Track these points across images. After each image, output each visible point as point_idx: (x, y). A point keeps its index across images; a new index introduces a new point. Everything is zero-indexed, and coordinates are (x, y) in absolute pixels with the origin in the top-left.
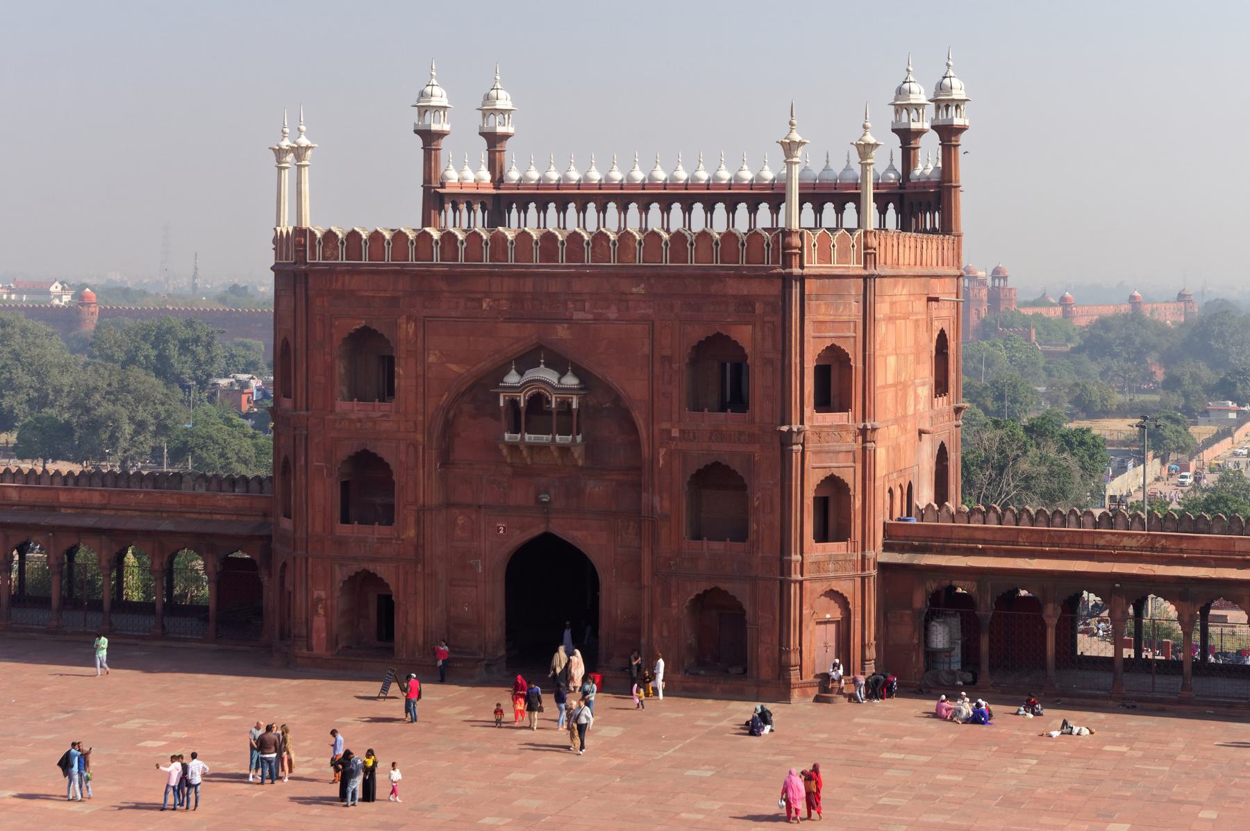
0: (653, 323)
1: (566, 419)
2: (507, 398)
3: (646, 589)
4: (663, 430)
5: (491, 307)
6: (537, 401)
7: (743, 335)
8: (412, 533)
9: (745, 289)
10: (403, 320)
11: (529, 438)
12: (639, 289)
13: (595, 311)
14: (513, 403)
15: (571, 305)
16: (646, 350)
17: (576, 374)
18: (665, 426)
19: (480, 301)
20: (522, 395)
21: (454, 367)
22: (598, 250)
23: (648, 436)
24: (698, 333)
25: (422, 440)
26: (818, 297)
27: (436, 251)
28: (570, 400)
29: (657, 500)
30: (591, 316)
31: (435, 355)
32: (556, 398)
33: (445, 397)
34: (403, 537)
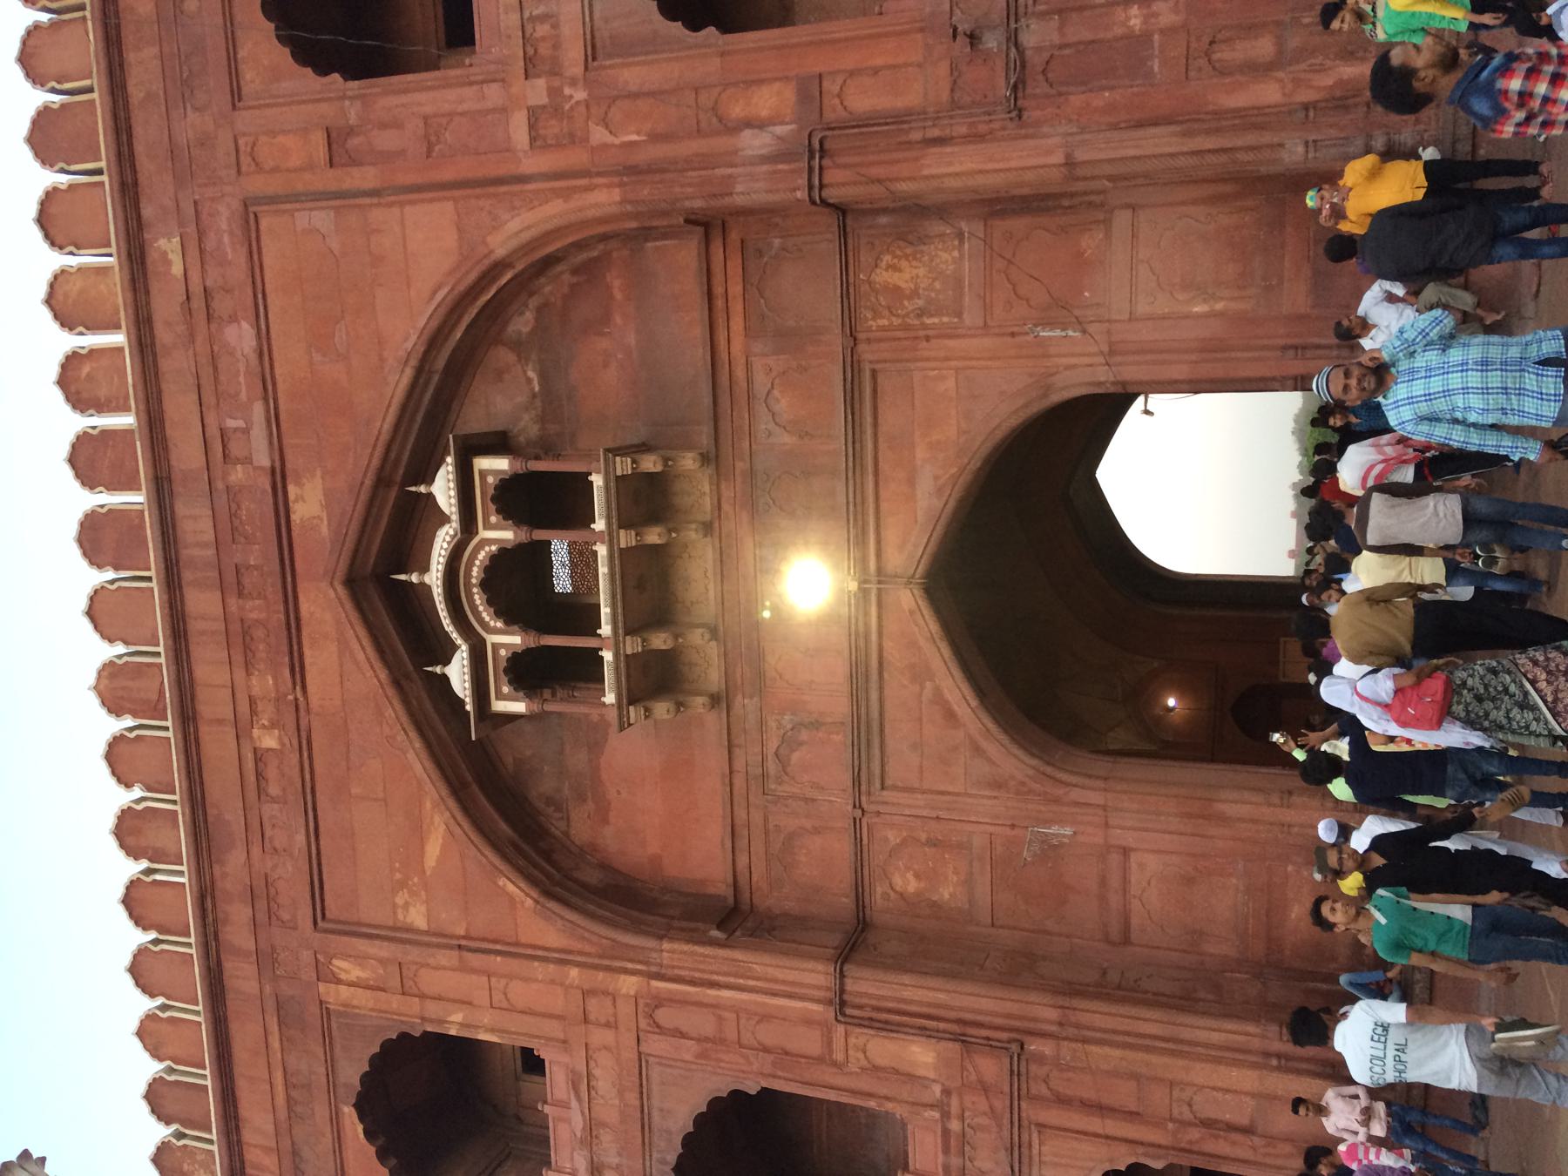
0: (258, 201)
2: (506, 689)
3: (1081, 155)
4: (533, 140)
5: (273, 725)
13: (243, 396)
15: (238, 474)
19: (259, 756)
20: (492, 639)
21: (433, 850)
22: (103, 392)
23: (556, 193)
25: (634, 979)
28: (490, 480)
29: (754, 143)
30: (258, 410)
31: (406, 906)
32: (488, 526)
33: (511, 887)
34: (937, 1089)
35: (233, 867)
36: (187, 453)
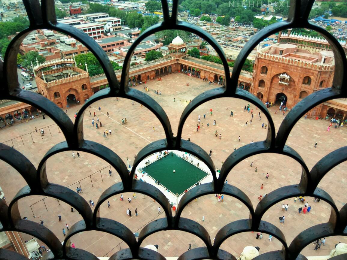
1: (287, 81)
6: (284, 79)
7: (312, 77)
8: (266, 90)
9: (313, 72)
10: (269, 66)
11: (282, 83)
12: (300, 69)
14: (281, 78)
16: (299, 76)
17: (289, 76)
18: (299, 85)
21: (275, 73)
24: (305, 76)
26: (323, 74)
27: (275, 59)
35: (275, 63)
36: (292, 67)
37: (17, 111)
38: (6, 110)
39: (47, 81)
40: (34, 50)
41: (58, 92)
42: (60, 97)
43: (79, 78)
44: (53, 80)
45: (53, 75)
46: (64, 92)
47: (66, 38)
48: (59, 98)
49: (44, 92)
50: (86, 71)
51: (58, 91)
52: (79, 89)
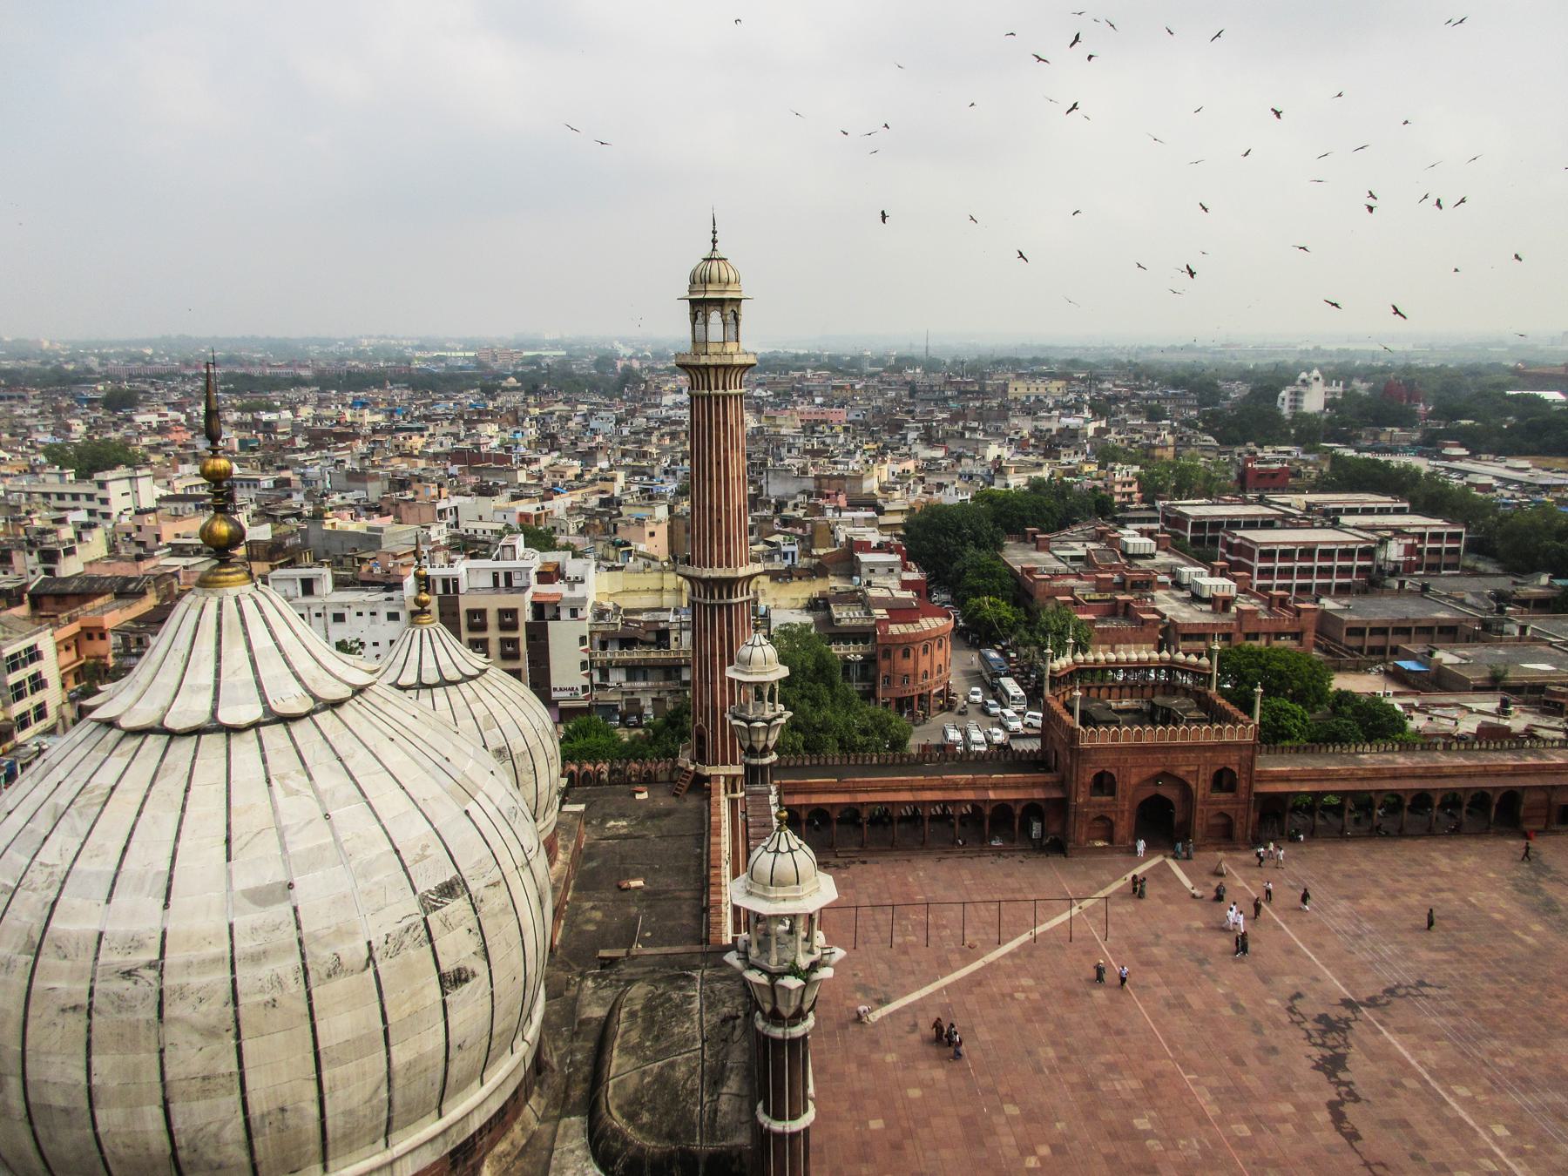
37: (945, 803)
38: (912, 789)
39: (1083, 723)
40: (1069, 598)
41: (1111, 775)
42: (1112, 793)
43: (1213, 740)
44: (1108, 723)
45: (1113, 705)
46: (1134, 780)
47: (1201, 574)
48: (1109, 798)
49: (1061, 758)
50: (1252, 717)
51: (1114, 771)
52: (1200, 787)
